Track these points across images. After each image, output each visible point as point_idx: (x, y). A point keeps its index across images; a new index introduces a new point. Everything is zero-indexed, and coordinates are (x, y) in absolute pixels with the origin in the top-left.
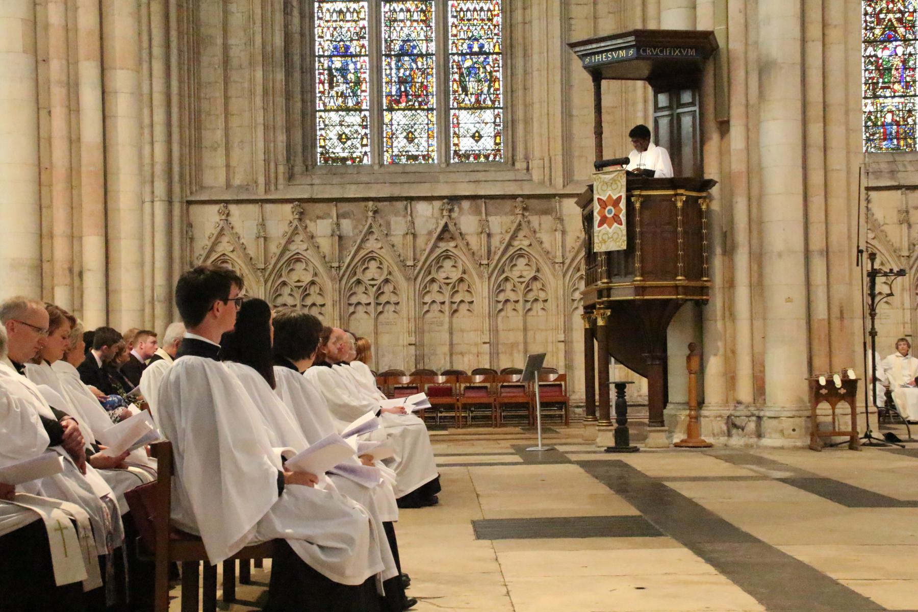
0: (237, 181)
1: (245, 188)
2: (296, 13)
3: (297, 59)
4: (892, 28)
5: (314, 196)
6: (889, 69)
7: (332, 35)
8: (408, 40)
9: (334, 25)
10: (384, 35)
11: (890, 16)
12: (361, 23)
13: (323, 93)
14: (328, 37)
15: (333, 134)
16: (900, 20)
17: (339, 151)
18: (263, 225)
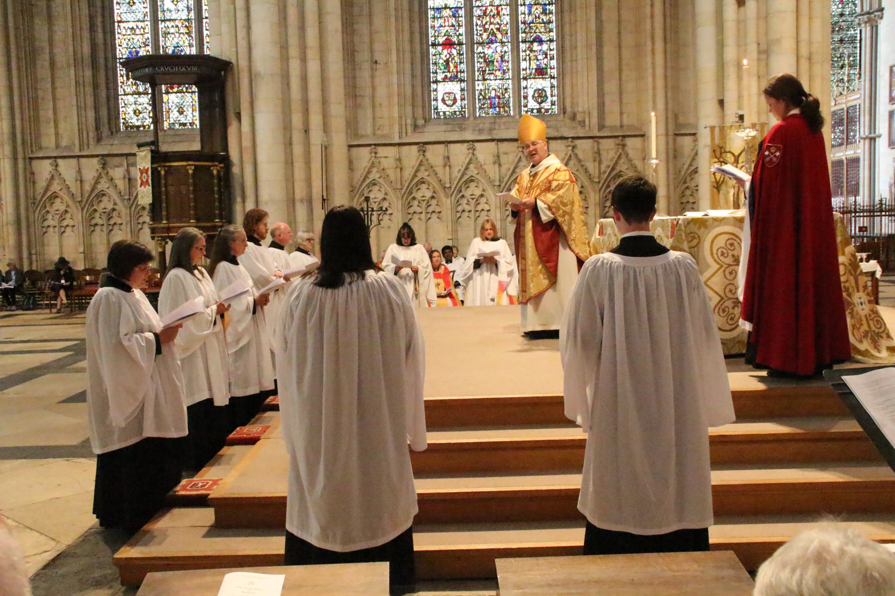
0: (64, 143)
1: (68, 148)
2: (100, 30)
3: (102, 61)
4: (494, 34)
5: (111, 153)
6: (493, 62)
7: (127, 44)
8: (178, 47)
9: (129, 37)
10: (161, 44)
11: (492, 26)
12: (146, 36)
13: (123, 83)
14: (125, 45)
15: (130, 110)
16: (498, 29)
17: (135, 121)
18: (79, 171)
